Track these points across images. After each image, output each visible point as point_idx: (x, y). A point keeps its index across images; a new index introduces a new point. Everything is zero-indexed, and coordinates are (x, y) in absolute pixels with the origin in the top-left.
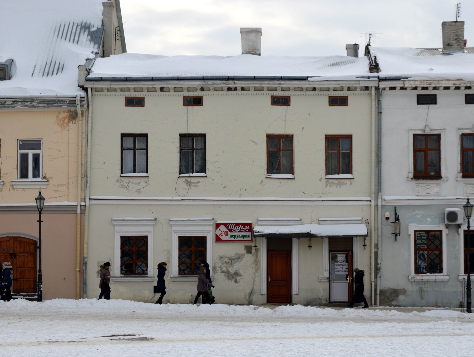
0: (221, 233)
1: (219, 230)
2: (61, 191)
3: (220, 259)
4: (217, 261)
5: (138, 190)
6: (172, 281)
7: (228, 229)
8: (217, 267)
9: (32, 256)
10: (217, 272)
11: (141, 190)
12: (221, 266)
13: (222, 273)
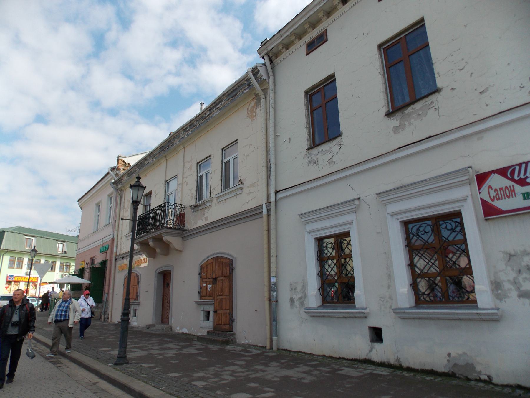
0: (494, 194)
1: (487, 188)
2: (253, 192)
3: (509, 261)
4: (501, 265)
5: (331, 160)
6: (400, 318)
7: (512, 180)
8: (504, 283)
9: (228, 280)
10: (506, 297)
11: (334, 159)
12: (515, 279)
13: (522, 299)
